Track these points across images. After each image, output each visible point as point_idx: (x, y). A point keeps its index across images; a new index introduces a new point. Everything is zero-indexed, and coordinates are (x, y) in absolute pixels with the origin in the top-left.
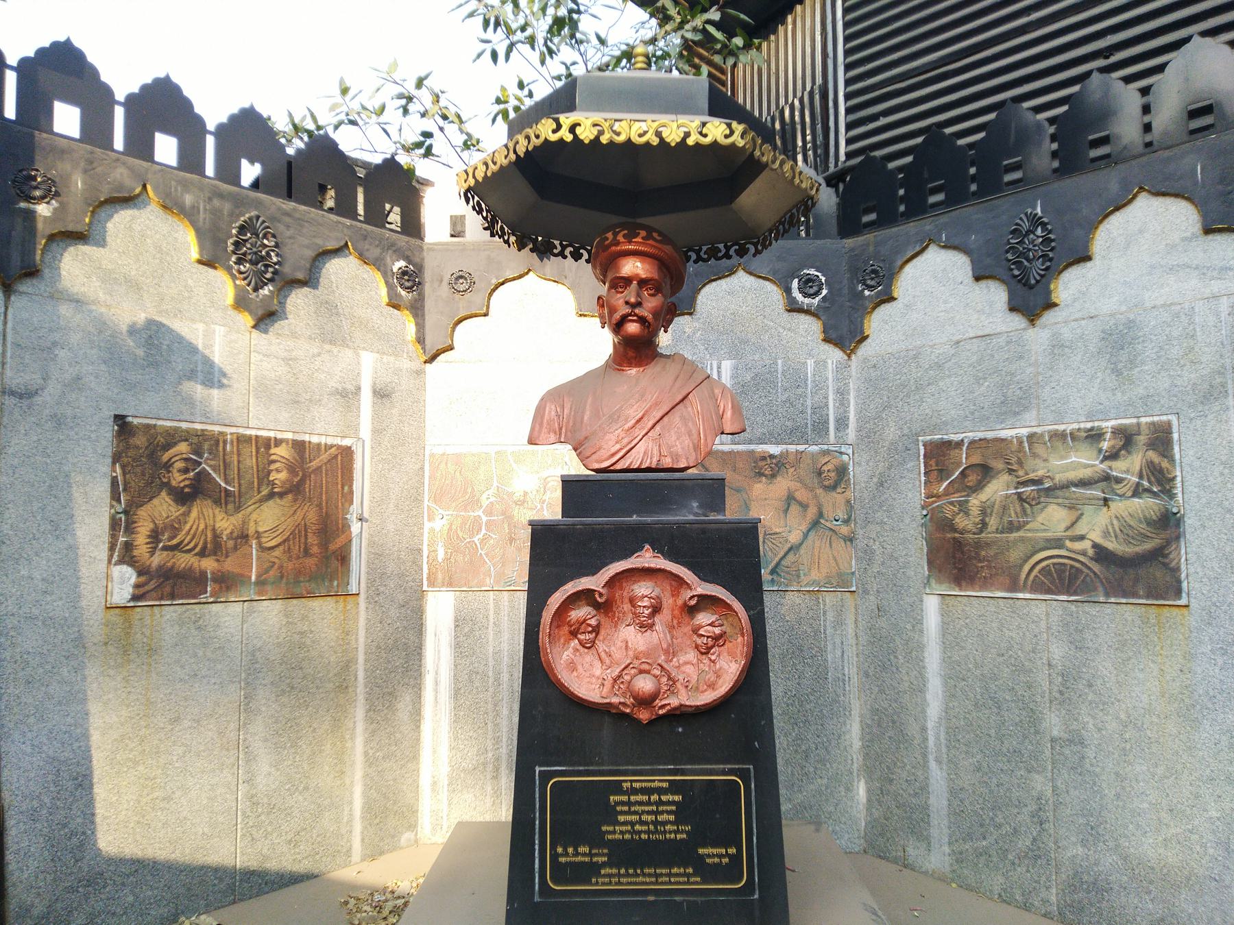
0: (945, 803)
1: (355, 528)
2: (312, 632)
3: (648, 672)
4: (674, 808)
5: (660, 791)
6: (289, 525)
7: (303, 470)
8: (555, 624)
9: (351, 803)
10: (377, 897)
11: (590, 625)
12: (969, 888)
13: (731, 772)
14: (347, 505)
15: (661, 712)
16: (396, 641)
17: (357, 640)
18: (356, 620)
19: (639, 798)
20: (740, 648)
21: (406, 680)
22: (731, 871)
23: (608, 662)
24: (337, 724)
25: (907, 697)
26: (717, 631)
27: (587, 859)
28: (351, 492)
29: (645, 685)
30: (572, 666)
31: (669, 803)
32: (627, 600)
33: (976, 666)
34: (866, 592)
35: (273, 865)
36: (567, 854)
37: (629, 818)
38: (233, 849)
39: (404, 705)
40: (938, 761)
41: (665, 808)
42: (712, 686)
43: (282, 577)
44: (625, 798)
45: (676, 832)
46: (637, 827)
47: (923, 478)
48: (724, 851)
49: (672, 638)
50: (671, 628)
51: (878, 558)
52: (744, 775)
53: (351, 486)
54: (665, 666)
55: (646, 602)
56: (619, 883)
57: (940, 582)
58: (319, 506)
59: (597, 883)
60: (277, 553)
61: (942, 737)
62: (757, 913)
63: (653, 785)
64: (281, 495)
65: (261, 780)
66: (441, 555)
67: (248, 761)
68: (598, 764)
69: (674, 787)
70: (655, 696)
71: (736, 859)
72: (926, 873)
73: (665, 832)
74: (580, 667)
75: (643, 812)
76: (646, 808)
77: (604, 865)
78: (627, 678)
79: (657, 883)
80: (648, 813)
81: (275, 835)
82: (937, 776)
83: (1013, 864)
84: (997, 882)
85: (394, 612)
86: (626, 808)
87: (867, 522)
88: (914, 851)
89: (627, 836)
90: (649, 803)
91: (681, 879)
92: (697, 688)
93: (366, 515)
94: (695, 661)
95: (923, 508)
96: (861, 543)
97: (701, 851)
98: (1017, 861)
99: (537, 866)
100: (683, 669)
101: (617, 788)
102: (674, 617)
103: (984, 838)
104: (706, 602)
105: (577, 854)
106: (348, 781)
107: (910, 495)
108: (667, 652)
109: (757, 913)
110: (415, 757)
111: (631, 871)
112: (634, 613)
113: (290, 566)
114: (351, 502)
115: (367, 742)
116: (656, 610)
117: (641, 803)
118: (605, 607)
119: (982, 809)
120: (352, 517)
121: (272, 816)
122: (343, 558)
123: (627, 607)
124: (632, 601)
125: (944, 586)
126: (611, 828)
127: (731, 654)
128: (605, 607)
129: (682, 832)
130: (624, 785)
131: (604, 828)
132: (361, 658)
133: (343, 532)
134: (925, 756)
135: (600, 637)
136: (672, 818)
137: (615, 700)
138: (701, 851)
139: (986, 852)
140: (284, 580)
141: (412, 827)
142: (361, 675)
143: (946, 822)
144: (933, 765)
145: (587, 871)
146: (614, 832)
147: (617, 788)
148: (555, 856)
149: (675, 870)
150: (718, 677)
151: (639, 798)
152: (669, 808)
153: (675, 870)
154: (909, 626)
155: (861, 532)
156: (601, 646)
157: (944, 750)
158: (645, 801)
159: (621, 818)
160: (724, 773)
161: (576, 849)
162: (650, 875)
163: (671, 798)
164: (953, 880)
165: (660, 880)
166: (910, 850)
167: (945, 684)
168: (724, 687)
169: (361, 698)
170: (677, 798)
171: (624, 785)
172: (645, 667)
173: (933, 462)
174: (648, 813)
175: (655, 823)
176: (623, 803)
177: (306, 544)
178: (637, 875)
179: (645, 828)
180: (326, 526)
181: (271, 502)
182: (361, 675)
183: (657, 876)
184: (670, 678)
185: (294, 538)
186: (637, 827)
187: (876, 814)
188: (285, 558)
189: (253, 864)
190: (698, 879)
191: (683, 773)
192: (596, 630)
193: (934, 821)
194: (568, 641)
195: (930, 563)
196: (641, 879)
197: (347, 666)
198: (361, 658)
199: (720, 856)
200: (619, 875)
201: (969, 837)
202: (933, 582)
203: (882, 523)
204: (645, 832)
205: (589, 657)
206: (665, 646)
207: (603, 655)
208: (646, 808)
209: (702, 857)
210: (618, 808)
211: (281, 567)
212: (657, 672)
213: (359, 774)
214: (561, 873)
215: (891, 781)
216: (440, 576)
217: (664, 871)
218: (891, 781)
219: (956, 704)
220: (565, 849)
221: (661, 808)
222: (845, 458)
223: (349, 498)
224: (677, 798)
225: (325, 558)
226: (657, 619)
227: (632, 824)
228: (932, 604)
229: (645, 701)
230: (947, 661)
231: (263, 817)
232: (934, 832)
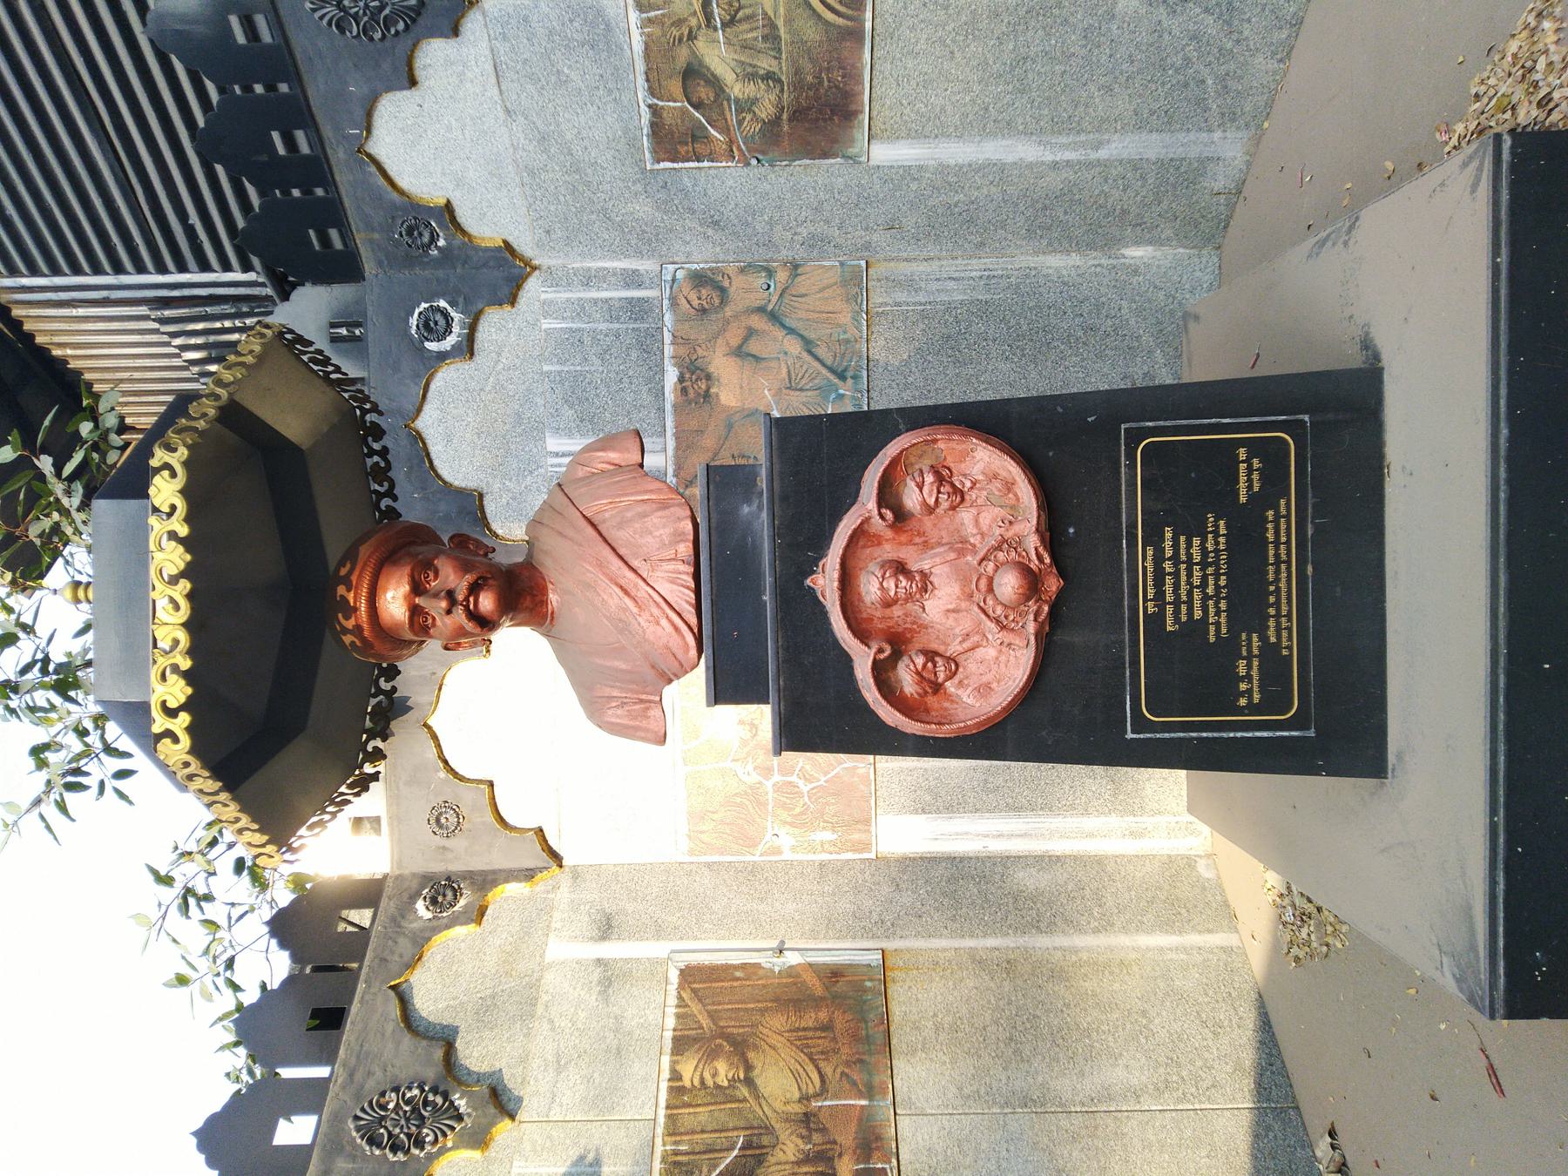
0: (1154, 135)
1: (792, 959)
2: (935, 1015)
3: (991, 580)
4: (1182, 538)
5: (1159, 559)
6: (789, 1054)
7: (714, 1038)
8: (924, 716)
9: (1161, 950)
10: (1288, 917)
11: (924, 666)
12: (1270, 105)
13: (1131, 456)
14: (761, 972)
15: (1048, 561)
16: (945, 894)
17: (945, 950)
18: (918, 952)
19: (1168, 589)
20: (953, 445)
21: (997, 877)
22: (1271, 455)
23: (976, 638)
24: (1057, 974)
25: (1010, 190)
26: (929, 478)
27: (1256, 663)
28: (743, 966)
29: (1009, 584)
30: (984, 690)
31: (1176, 546)
32: (888, 611)
33: (968, 91)
34: (867, 246)
35: (1248, 1057)
36: (1249, 692)
37: (1197, 604)
38: (1227, 1113)
39: (1028, 880)
40: (1098, 146)
41: (1182, 552)
42: (1009, 486)
43: (861, 1061)
44: (1169, 609)
45: (1216, 534)
46: (1210, 591)
47: (706, 164)
48: (1243, 466)
49: (940, 544)
50: (926, 546)
51: (820, 228)
52: (1135, 437)
53: (736, 967)
54: (981, 554)
55: (890, 584)
56: (1289, 616)
57: (852, 141)
58: (763, 1011)
59: (1290, 648)
60: (828, 1070)
61: (1063, 140)
62: (1331, 416)
63: (1150, 569)
64: (749, 1068)
65: (1137, 1079)
66: (828, 836)
67: (1110, 1098)
68: (1123, 650)
69: (1153, 538)
70: (1025, 570)
71: (1255, 447)
72: (1249, 164)
73: (1217, 551)
74: (985, 679)
75: (1189, 583)
76: (1183, 578)
77: (1264, 638)
78: (999, 610)
79: (1289, 562)
80: (1190, 575)
81: (1206, 1055)
82: (1120, 147)
83: (1238, 41)
84: (1262, 64)
85: (906, 898)
86: (1184, 608)
87: (769, 244)
88: (1220, 180)
89: (1223, 605)
90: (1176, 575)
91: (1283, 527)
92: (1012, 507)
93: (774, 944)
94: (974, 511)
95: (748, 164)
96: (800, 253)
97: (1243, 499)
98: (1235, 36)
99: (1265, 734)
100: (985, 529)
101: (1155, 621)
102: (910, 543)
103: (1203, 82)
104: (888, 495)
105: (1249, 677)
106: (1133, 956)
107: (730, 183)
108: (961, 553)
109: (1331, 416)
110: (1099, 861)
111: (1272, 599)
112: (906, 600)
113: (845, 1050)
114: (757, 966)
115: (1080, 931)
116: (900, 568)
117: (1176, 587)
118: (898, 643)
119: (1163, 84)
120: (778, 963)
121: (1182, 1060)
122: (835, 974)
123: (897, 611)
124: (888, 603)
125: (858, 135)
126: (1212, 629)
127: (963, 456)
128: (898, 643)
129: (1217, 527)
130: (1151, 610)
131: (1212, 639)
132: (969, 943)
133: (798, 976)
134: (1090, 165)
135: (941, 649)
136: (1196, 541)
137: (1031, 627)
138: (1243, 499)
139: (1222, 80)
140: (865, 1057)
141: (1190, 862)
142: (991, 942)
143: (1181, 136)
144: (1103, 154)
145: (1273, 662)
146: (1218, 623)
147: (1155, 621)
148: (1252, 708)
149: (1270, 536)
150: (995, 476)
151: (1168, 589)
152: (1183, 545)
153: (1270, 536)
154: (914, 186)
155: (784, 252)
156: (954, 648)
157: (1083, 137)
158: (1172, 579)
159: (1198, 614)
160: (1132, 466)
161: (1242, 679)
162: (1277, 572)
163: (1168, 544)
164: (1259, 127)
165: (1284, 557)
166: (1218, 186)
167: (993, 135)
168: (1010, 468)
169: (1022, 941)
170: (1168, 535)
171: (1151, 610)
172: (983, 584)
173: (683, 150)
174: (1190, 575)
175: (1204, 565)
176: (1177, 613)
177: (816, 1029)
178: (1278, 589)
179: (1211, 581)
180: (790, 1000)
181: (758, 1082)
182: (991, 942)
183: (1278, 562)
184: (999, 548)
185: (808, 1046)
186: (1210, 591)
187: (1169, 233)
188: (835, 1059)
189: (1248, 1084)
190: (1283, 502)
191: (1132, 526)
192: (931, 655)
193: (1180, 152)
194: (948, 697)
195: (825, 155)
196: (1283, 585)
197: (979, 962)
198: (969, 943)
199: (1250, 470)
200: (1278, 616)
201: (1200, 102)
202: (852, 151)
203: (771, 223)
204: (1217, 580)
205: (971, 666)
206: (952, 555)
207: (966, 645)
208: (1183, 578)
209: (1252, 497)
210: (1184, 619)
211: (848, 1064)
212: (991, 566)
213: (1124, 940)
214: (1275, 700)
215: (1124, 212)
216: (856, 836)
217: (1271, 553)
218: (1124, 212)
219: (1020, 120)
220: (1242, 694)
221: (1183, 558)
222: (680, 274)
223: (751, 969)
224: (1168, 535)
225: (836, 1000)
226: (914, 567)
227: (1206, 597)
228: (883, 153)
229: (1032, 582)
230: (961, 132)
231: (1184, 1073)
232: (1194, 152)
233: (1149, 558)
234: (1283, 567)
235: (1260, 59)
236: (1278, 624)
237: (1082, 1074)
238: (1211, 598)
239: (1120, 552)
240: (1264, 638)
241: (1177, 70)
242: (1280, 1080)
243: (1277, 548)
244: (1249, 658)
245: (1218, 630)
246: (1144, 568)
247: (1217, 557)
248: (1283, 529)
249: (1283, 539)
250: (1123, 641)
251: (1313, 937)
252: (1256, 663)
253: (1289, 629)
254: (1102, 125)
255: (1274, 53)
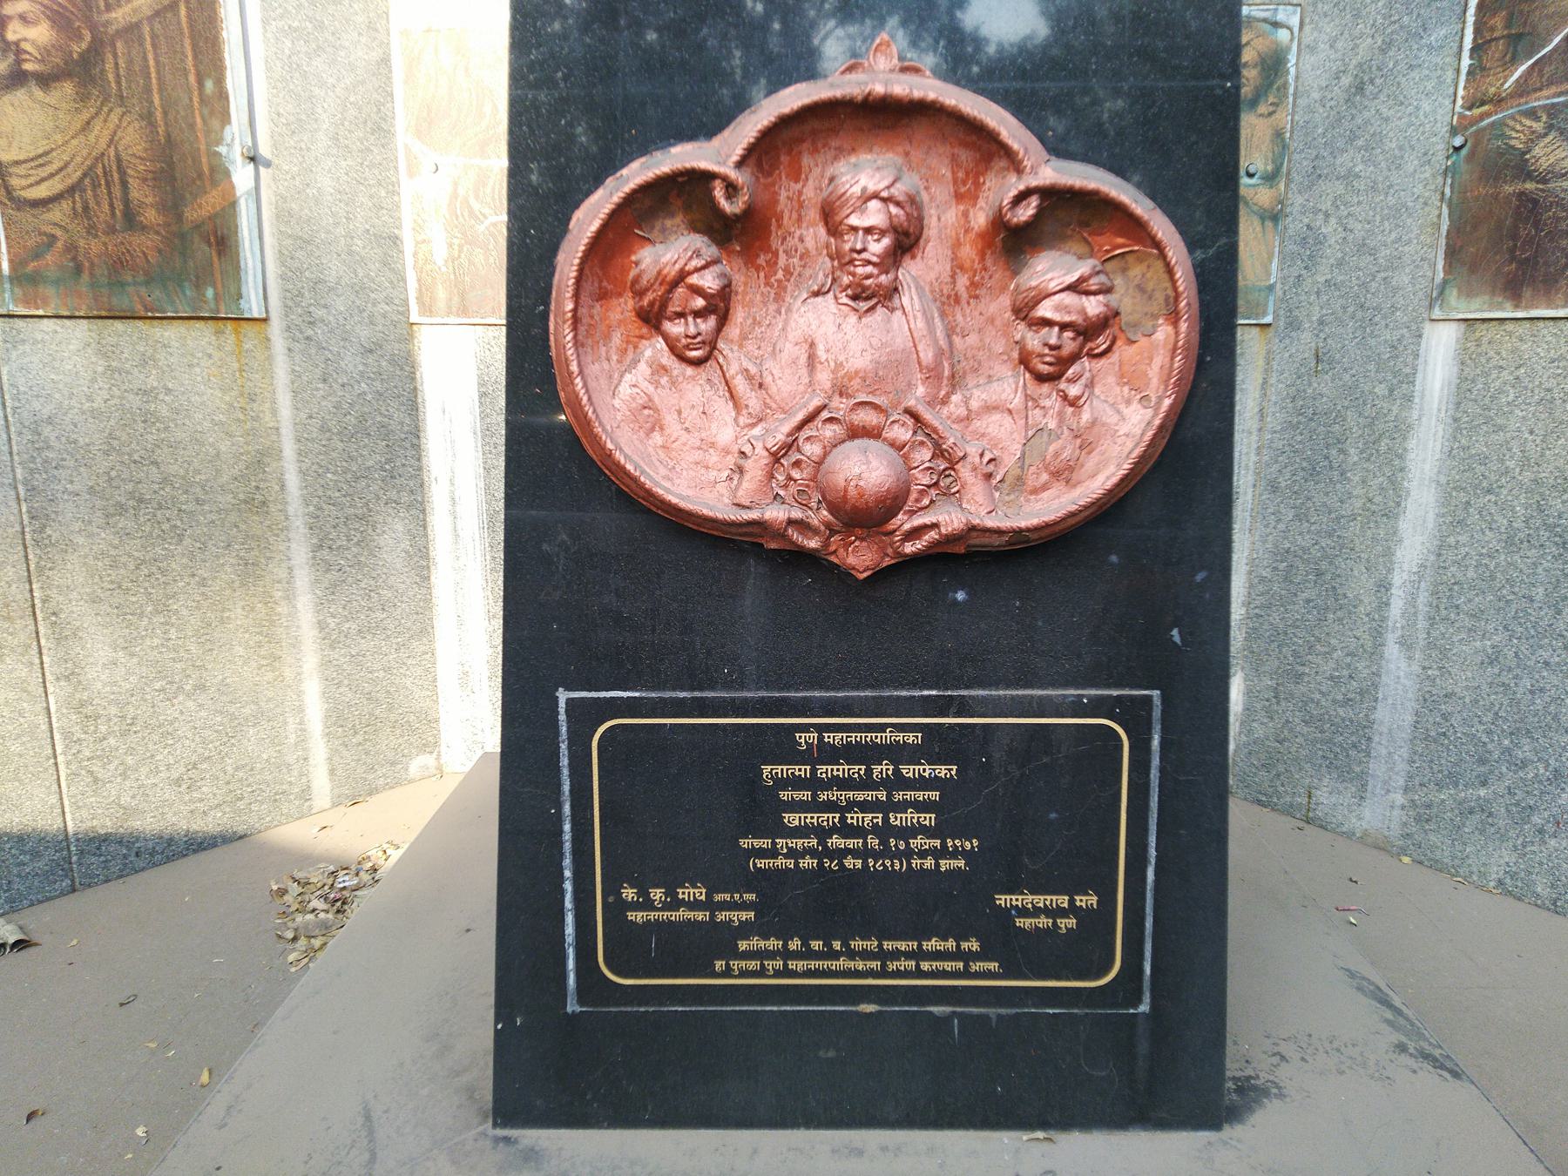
0: (1409, 719)
1: (242, 177)
2: (168, 391)
3: (873, 433)
4: (935, 795)
5: (897, 753)
6: (78, 152)
7: (93, 28)
8: (589, 287)
9: (301, 710)
10: (345, 880)
11: (697, 291)
12: (1437, 866)
13: (1096, 707)
15: (909, 548)
16: (362, 419)
17: (274, 412)
18: (268, 370)
19: (841, 770)
20: (1160, 360)
21: (393, 494)
22: (1086, 945)
23: (753, 400)
24: (250, 570)
25: (1355, 527)
26: (1093, 306)
27: (700, 916)
28: (223, 96)
29: (865, 470)
30: (649, 417)
31: (922, 783)
32: (813, 214)
33: (1525, 463)
34: (1294, 325)
35: (147, 823)
36: (648, 905)
37: (812, 818)
38: (54, 799)
39: (392, 535)
40: (1406, 644)
41: (910, 795)
42: (1064, 474)
43: (78, 269)
44: (802, 771)
45: (939, 854)
46: (836, 841)
47: (1466, 62)
48: (1063, 901)
49: (950, 331)
50: (949, 301)
51: (1331, 252)
52: (1134, 715)
53: (220, 82)
54: (927, 415)
55: (874, 215)
56: (786, 973)
57: (1468, 293)
58: (148, 117)
59: (727, 973)
60: (57, 214)
61: (1423, 598)
62: (1143, 1047)
63: (879, 738)
64: (45, 80)
65: (97, 677)
66: (440, 254)
67: (59, 640)
68: (728, 686)
69: (938, 745)
70: (893, 502)
71: (1096, 924)
72: (1349, 835)
73: (908, 854)
74: (670, 419)
75: (851, 805)
76: (861, 796)
77: (745, 930)
78: (812, 450)
79: (883, 974)
80: (865, 807)
81: (144, 771)
82: (1400, 672)
83: (1541, 831)
84: (1500, 859)
85: (351, 362)
86: (805, 795)
87: (1315, 176)
88: (1329, 797)
89: (808, 863)
90: (867, 783)
91: (948, 966)
92: (1020, 480)
93: (265, 150)
94: (1017, 401)
95: (1454, 131)
96: (1294, 224)
97: (1002, 900)
98: (1550, 828)
99: (570, 930)
100: (976, 424)
101: (782, 746)
102: (958, 266)
103: (1484, 784)
104: (1067, 213)
105: (675, 904)
106: (288, 673)
107: (1426, 106)
108: (932, 374)
109: (1143, 1047)
110: (425, 630)
111: (816, 945)
112: (836, 256)
113: (95, 246)
114: (225, 118)
115: (320, 605)
116: (905, 242)
117: (845, 784)
118: (744, 234)
119: (1489, 733)
121: (132, 738)
122: (222, 240)
123: (814, 235)
124: (830, 216)
125: (1477, 302)
126: (765, 843)
127: (1132, 380)
128: (744, 234)
129: (954, 854)
130: (802, 738)
131: (745, 843)
132: (289, 449)
134: (1378, 634)
135: (732, 331)
136: (928, 819)
137: (776, 514)
138: (1002, 900)
139: (1484, 808)
140: (85, 277)
141: (430, 746)
142: (293, 480)
143: (1404, 752)
144: (1392, 650)
145: (699, 946)
146: (782, 854)
147: (782, 746)
148: (616, 910)
149: (932, 944)
150: (1086, 446)
151: (841, 770)
152: (921, 796)
153: (932, 944)
154: (1381, 390)
155: (1299, 200)
156: (733, 357)
157: (1422, 624)
158: (863, 776)
159: (793, 819)
160: (1077, 709)
161: (671, 892)
162: (866, 955)
163: (927, 770)
164: (1403, 851)
165: (892, 966)
166: (1323, 796)
167: (1446, 500)
168: (1102, 476)
169: (299, 525)
170: (942, 771)
171: (802, 738)
172: (867, 417)
173: (1498, 21)
174: (865, 807)
175: (884, 831)
176: (796, 783)
177: (126, 202)
178: (835, 955)
179: (851, 843)
180: (171, 165)
182: (293, 480)
183: (883, 956)
184: (939, 452)
185: (95, 186)
186: (836, 841)
187: (1260, 732)
188: (77, 228)
189: (105, 823)
190: (993, 966)
191: (963, 708)
192: (719, 306)
193: (1380, 748)
194: (632, 342)
195: (1452, 253)
196: (842, 963)
197: (262, 460)
198: (289, 449)
199: (1060, 912)
200: (786, 955)
201: (1453, 779)
202: (1452, 295)
203: (1349, 177)
204: (854, 853)
205: (696, 389)
206: (927, 356)
207: (740, 384)
208: (861, 796)
209: (1006, 914)
210: (785, 795)
211: (71, 248)
212: (902, 433)
213: (310, 660)
214: (630, 947)
215: (1299, 677)
216: (441, 294)
217: (902, 946)
218: (1299, 677)
219: (1463, 539)
220: (643, 892)
221: (898, 796)
222: (1283, 35)
223: (219, 105)
224: (942, 771)
225: (178, 238)
226: (911, 271)
227: (822, 833)
228: (1441, 344)
229: (865, 517)
230: (1458, 453)
231: (112, 741)
232: (1377, 768)
233: (900, 737)
234: (875, 965)
235: (1508, 856)
236: (772, 955)
237: (95, 600)
238: (822, 842)
239: (914, 685)
240: (745, 930)
241: (1508, 750)
242: (115, 868)
243: (909, 955)
244: (709, 905)
245: (762, 853)
246: (882, 728)
247: (898, 855)
248: (941, 965)
249: (925, 966)
250: (742, 687)
251: (310, 917)
252: (700, 916)
253: (761, 973)
254: (1438, 651)
255: (1513, 876)
